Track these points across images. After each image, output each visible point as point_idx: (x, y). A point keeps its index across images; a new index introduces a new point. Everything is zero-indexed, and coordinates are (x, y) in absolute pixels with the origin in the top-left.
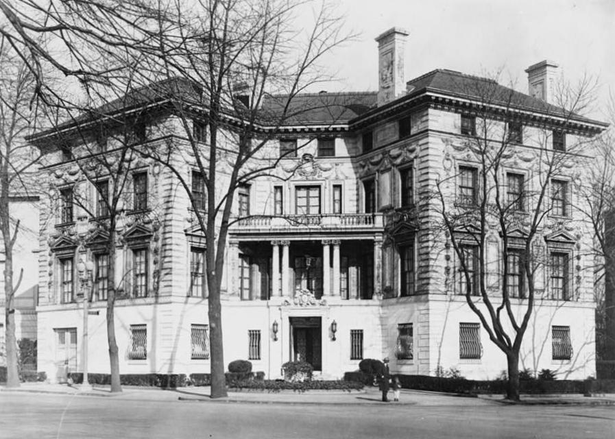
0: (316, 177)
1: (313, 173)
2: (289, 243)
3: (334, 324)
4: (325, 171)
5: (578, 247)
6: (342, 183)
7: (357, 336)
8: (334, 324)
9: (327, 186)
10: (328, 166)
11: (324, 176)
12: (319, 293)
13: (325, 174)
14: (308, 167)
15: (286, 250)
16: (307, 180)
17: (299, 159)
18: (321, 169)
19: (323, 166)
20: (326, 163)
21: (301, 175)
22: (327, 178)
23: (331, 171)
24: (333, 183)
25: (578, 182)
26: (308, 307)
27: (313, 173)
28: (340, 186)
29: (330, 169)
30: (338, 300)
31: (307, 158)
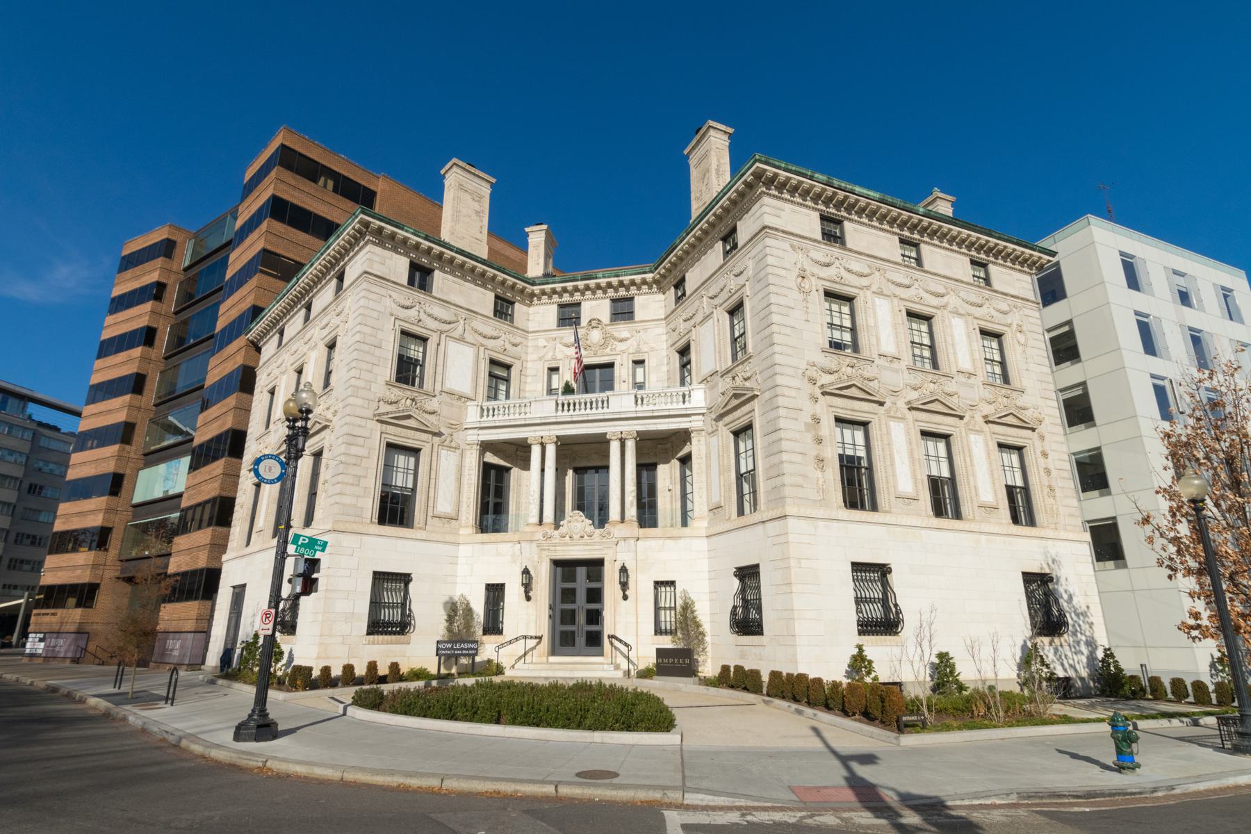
0: (608, 351)
3: (624, 570)
4: (622, 340)
5: (1042, 437)
6: (645, 357)
8: (624, 570)
9: (625, 364)
10: (625, 334)
12: (601, 519)
13: (621, 347)
14: (596, 336)
16: (595, 355)
18: (614, 338)
19: (616, 335)
20: (622, 329)
23: (628, 342)
25: (1021, 338)
26: (583, 541)
27: (604, 345)
28: (642, 362)
30: (632, 529)
31: (595, 323)
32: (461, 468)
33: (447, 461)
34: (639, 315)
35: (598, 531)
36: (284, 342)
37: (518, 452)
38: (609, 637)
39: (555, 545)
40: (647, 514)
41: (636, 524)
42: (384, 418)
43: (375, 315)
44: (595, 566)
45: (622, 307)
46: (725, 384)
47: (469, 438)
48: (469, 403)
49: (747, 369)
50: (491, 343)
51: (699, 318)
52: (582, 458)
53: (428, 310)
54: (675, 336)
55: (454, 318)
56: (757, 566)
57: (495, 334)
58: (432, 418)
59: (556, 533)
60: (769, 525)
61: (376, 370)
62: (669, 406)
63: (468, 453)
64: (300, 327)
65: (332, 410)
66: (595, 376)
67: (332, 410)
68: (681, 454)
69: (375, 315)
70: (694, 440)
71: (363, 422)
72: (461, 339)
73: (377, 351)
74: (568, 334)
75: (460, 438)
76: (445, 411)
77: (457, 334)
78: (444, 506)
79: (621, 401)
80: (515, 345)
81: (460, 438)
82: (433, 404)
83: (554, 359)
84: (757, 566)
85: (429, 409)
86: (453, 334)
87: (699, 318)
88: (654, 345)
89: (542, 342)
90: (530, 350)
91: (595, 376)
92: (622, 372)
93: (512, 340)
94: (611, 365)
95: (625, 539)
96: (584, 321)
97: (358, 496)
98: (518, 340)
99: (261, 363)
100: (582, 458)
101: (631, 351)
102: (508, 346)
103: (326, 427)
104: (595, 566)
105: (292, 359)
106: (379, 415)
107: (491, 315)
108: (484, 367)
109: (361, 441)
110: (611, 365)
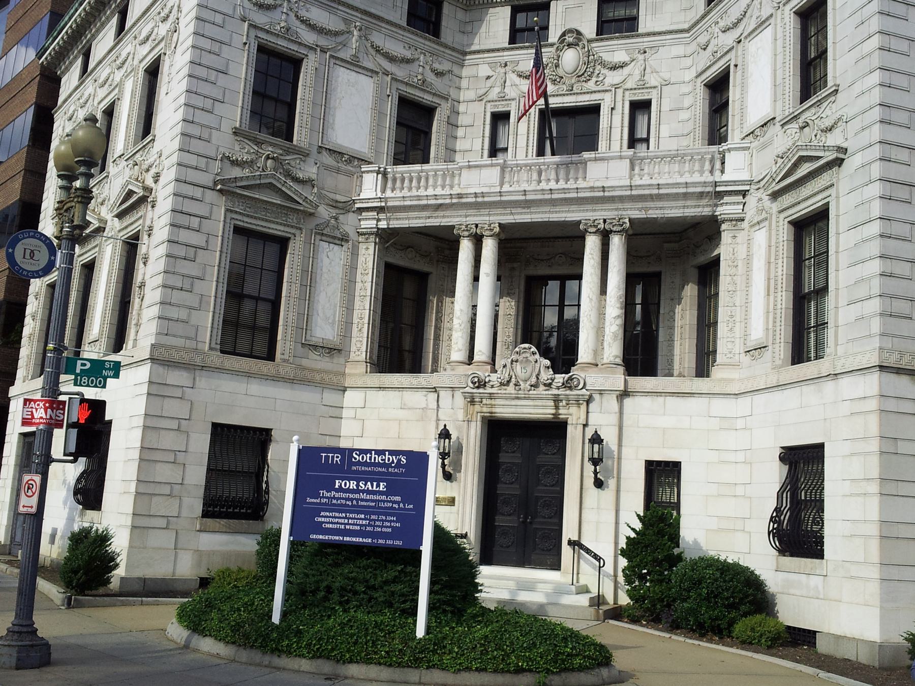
0: (591, 85)
1: (583, 75)
2: (497, 230)
3: (596, 439)
4: (614, 68)
6: (654, 96)
7: (662, 475)
10: (620, 56)
11: (608, 81)
13: (613, 78)
14: (570, 58)
15: (489, 248)
16: (570, 92)
17: (552, 45)
18: (603, 64)
19: (607, 57)
20: (615, 50)
21: (554, 82)
22: (617, 87)
23: (626, 70)
24: (629, 97)
27: (583, 75)
29: (622, 66)
32: (352, 268)
33: (332, 259)
34: (645, 24)
35: (560, 378)
36: (91, 66)
37: (443, 245)
38: (571, 543)
39: (491, 396)
40: (642, 355)
41: (621, 369)
42: (231, 187)
43: (219, 19)
44: (553, 432)
45: (621, 12)
46: (782, 140)
47: (364, 224)
48: (365, 168)
49: (829, 113)
50: (400, 72)
51: (750, 23)
52: (538, 261)
53: (303, 13)
54: (704, 59)
55: (341, 27)
56: (820, 447)
57: (408, 54)
58: (305, 191)
59: (494, 377)
60: (845, 381)
61: (219, 108)
62: (687, 178)
63: (362, 247)
64: (112, 44)
65: (153, 171)
66: (569, 130)
67: (153, 171)
68: (702, 259)
69: (219, 19)
70: (726, 237)
71: (198, 193)
72: (354, 64)
73: (222, 80)
74: (525, 59)
75: (349, 223)
76: (330, 181)
77: (346, 54)
78: (324, 330)
79: (608, 168)
80: (439, 74)
81: (349, 223)
82: (309, 170)
83: (503, 98)
84: (820, 447)
85: (300, 175)
86: (341, 55)
87: (750, 23)
88: (666, 76)
89: (484, 70)
90: (464, 83)
91: (569, 130)
92: (613, 125)
93: (436, 66)
94: (594, 110)
95: (601, 392)
96: (554, 36)
97: (191, 308)
98: (444, 66)
99: (59, 103)
100: (538, 261)
101: (629, 85)
102: (431, 77)
103: (143, 200)
104: (553, 432)
105: (101, 93)
106: (223, 182)
107: (404, 23)
108: (390, 108)
109: (195, 222)
110: (594, 110)
